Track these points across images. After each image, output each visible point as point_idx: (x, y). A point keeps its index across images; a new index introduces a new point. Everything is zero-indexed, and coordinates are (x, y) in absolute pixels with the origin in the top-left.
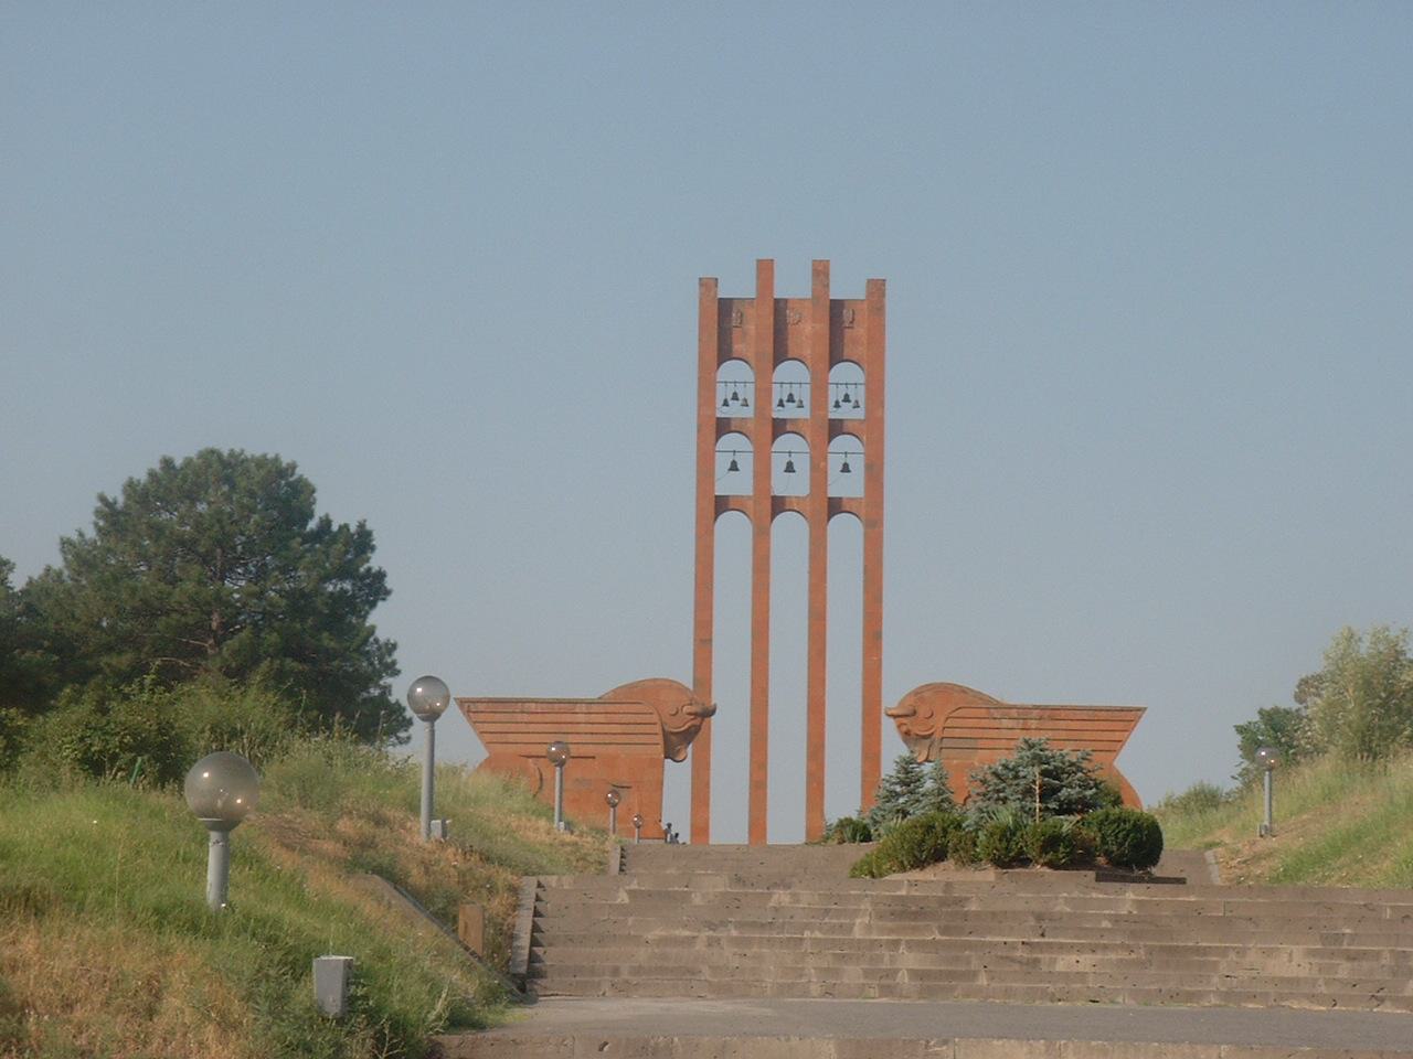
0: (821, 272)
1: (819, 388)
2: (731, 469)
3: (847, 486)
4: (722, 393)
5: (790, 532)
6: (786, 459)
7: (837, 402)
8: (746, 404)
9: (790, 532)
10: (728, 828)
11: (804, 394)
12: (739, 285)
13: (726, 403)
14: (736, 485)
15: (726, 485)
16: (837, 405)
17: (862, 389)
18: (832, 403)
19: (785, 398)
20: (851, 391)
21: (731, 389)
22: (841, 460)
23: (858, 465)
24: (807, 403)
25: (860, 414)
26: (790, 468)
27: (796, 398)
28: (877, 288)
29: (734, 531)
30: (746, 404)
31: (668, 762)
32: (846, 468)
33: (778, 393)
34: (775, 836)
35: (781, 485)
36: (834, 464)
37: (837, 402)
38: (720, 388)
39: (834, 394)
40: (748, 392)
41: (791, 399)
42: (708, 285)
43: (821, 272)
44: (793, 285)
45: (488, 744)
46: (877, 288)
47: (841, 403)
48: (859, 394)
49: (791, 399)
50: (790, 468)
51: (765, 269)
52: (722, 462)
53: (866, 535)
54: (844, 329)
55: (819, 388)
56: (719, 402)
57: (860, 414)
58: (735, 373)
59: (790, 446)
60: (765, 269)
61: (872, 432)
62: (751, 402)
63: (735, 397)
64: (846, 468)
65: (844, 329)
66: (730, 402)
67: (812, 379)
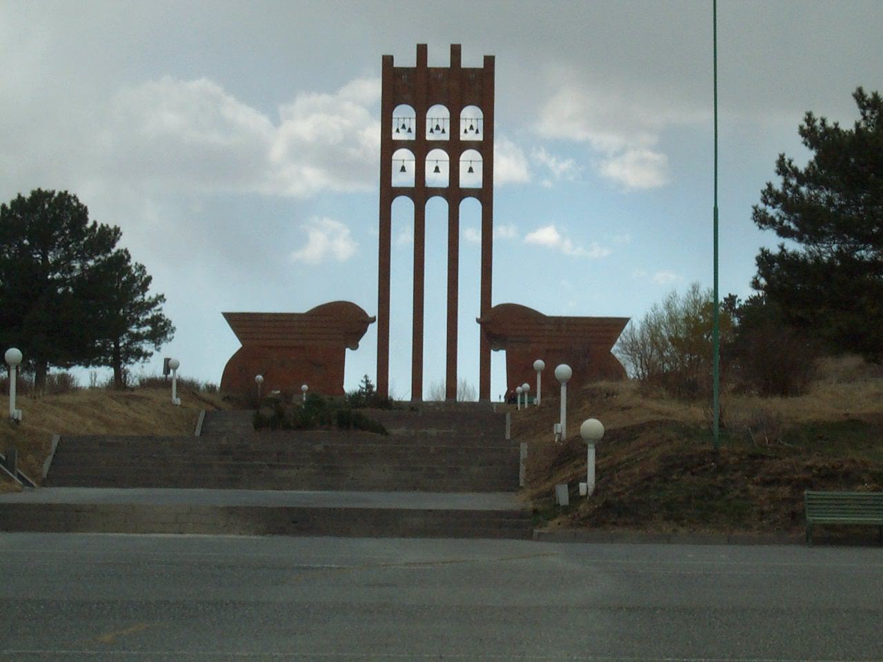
0: (456, 51)
5: (437, 208)
9: (437, 208)
10: (400, 390)
12: (406, 59)
14: (403, 179)
17: (482, 121)
19: (434, 128)
24: (447, 130)
25: (480, 137)
26: (437, 170)
27: (441, 129)
28: (489, 61)
29: (403, 208)
31: (348, 350)
32: (471, 170)
34: (426, 397)
39: (464, 125)
42: (387, 61)
43: (456, 51)
44: (439, 59)
45: (241, 340)
46: (489, 61)
47: (468, 131)
49: (438, 128)
51: (422, 50)
53: (483, 209)
54: (470, 86)
56: (394, 130)
57: (480, 137)
58: (404, 115)
60: (422, 50)
61: (486, 148)
64: (471, 170)
65: (470, 86)
66: (400, 130)
67: (450, 116)
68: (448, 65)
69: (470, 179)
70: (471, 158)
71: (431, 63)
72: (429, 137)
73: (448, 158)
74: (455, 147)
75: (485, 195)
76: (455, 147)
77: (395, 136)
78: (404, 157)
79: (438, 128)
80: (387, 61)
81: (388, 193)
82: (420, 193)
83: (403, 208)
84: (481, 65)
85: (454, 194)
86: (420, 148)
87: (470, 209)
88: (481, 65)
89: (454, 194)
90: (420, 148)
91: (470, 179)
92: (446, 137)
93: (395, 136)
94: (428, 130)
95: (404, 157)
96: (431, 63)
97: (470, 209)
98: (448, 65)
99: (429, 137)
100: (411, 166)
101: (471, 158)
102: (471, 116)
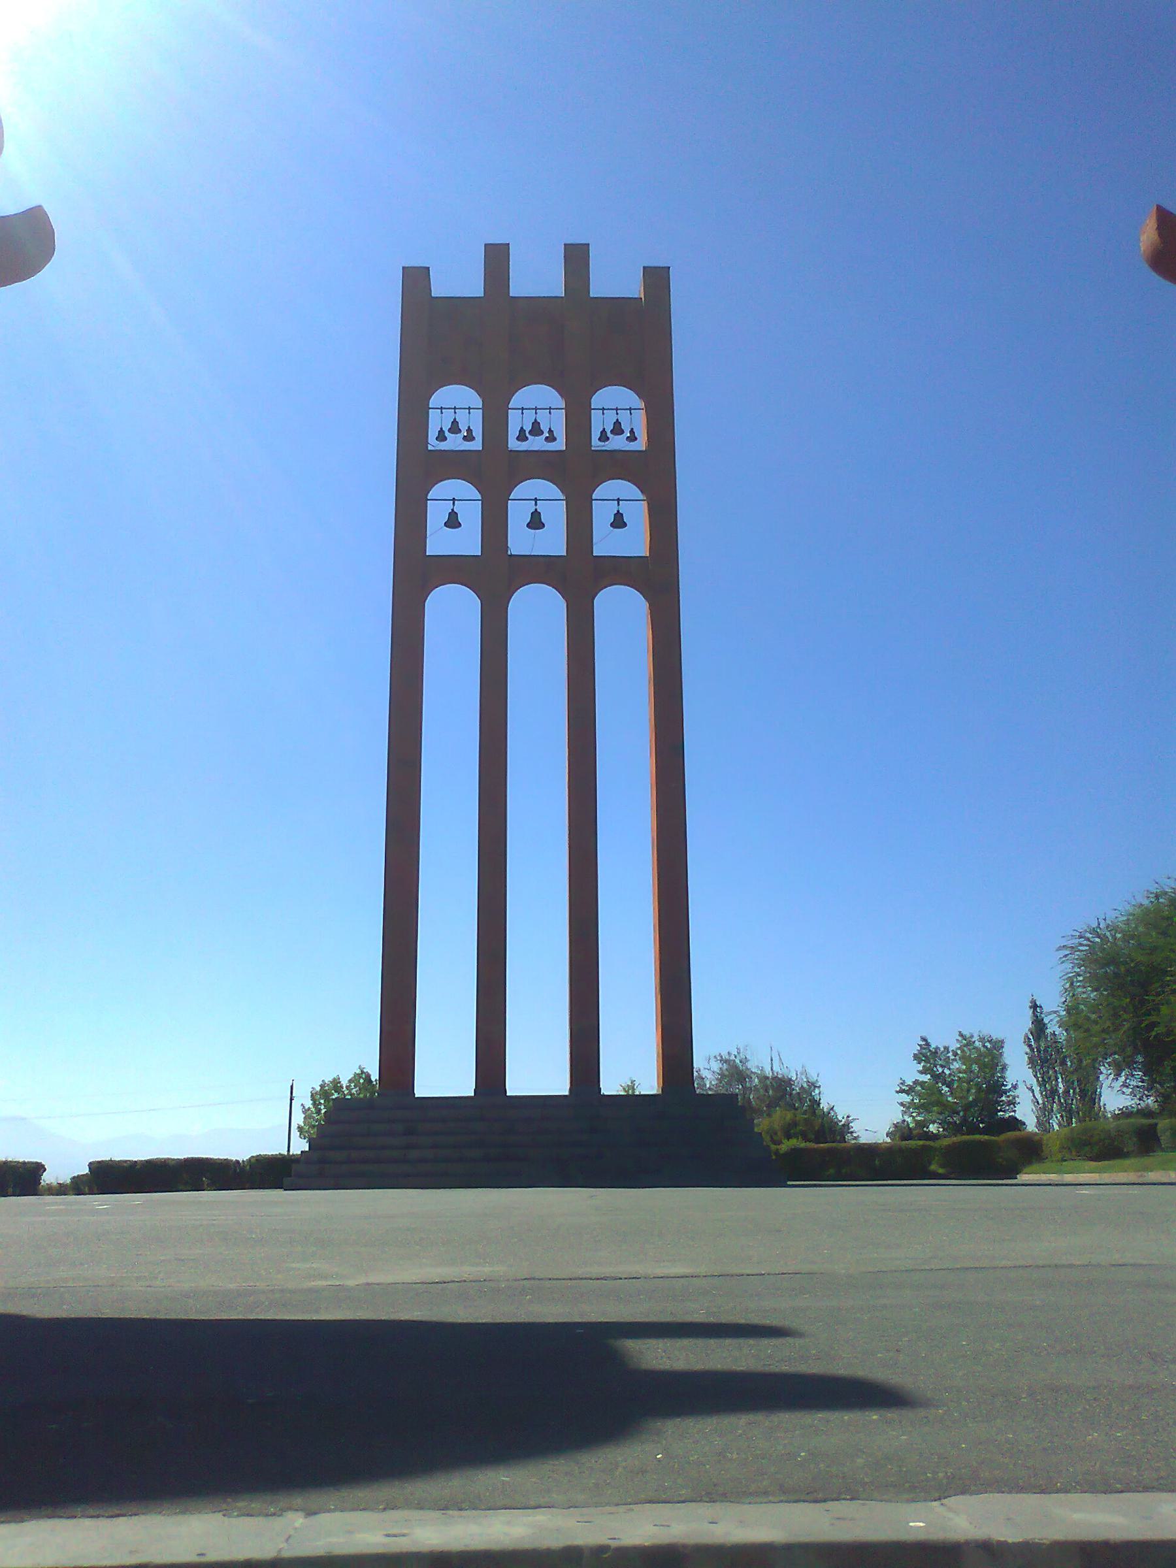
0: (577, 258)
3: (623, 537)
4: (436, 422)
5: (537, 613)
8: (469, 437)
9: (537, 613)
11: (557, 422)
12: (459, 279)
14: (454, 538)
15: (440, 542)
16: (604, 437)
19: (528, 428)
20: (624, 417)
21: (449, 417)
22: (613, 508)
23: (638, 513)
26: (536, 522)
27: (544, 427)
29: (452, 613)
30: (469, 437)
33: (515, 422)
35: (521, 541)
36: (602, 514)
38: (433, 415)
39: (599, 422)
40: (475, 422)
42: (415, 280)
43: (577, 258)
44: (537, 277)
46: (657, 279)
49: (536, 430)
50: (536, 522)
51: (497, 258)
52: (436, 514)
58: (456, 406)
60: (497, 258)
61: (654, 471)
62: (478, 433)
63: (455, 428)
66: (447, 434)
69: (623, 537)
72: (513, 444)
74: (578, 470)
75: (656, 575)
76: (578, 470)
77: (433, 444)
78: (453, 495)
79: (536, 430)
80: (415, 280)
81: (416, 574)
82: (495, 576)
83: (452, 613)
84: (632, 287)
85: (579, 576)
86: (495, 471)
87: (621, 613)
89: (579, 576)
90: (495, 471)
92: (560, 444)
93: (433, 444)
94: (513, 432)
95: (453, 495)
97: (621, 613)
99: (513, 444)
100: (472, 515)
102: (617, 408)
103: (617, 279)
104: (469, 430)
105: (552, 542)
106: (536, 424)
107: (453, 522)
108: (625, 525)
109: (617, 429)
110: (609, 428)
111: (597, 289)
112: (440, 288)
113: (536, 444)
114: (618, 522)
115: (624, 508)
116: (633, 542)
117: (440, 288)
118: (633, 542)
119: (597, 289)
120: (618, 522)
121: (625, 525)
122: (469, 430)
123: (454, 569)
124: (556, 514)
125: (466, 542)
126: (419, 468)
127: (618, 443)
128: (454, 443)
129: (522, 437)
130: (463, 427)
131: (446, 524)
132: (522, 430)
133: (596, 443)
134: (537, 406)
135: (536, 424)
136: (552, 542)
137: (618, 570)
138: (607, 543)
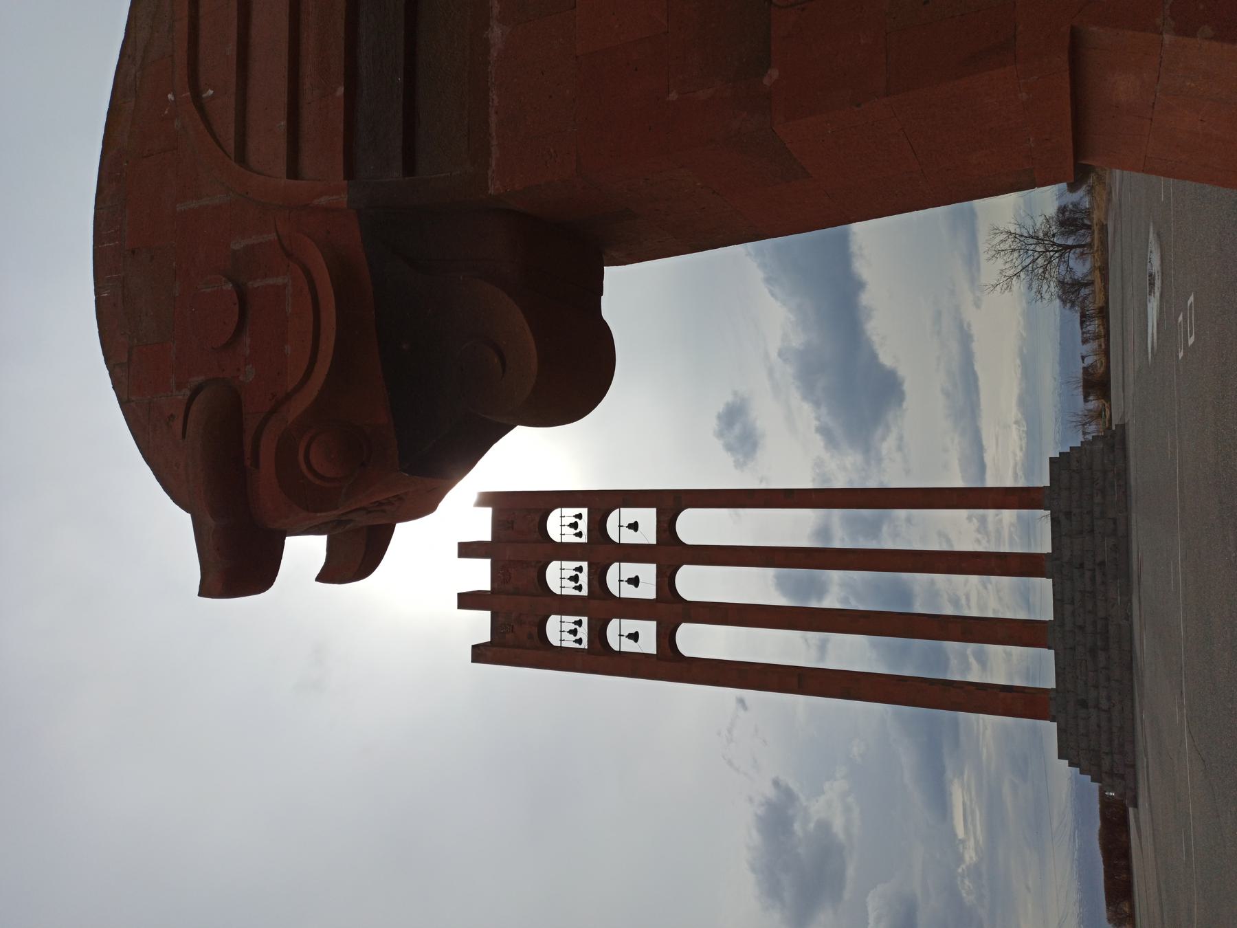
0: (468, 550)
1: (566, 552)
2: (636, 641)
5: (694, 583)
6: (624, 584)
7: (576, 535)
8: (579, 623)
9: (694, 583)
12: (479, 625)
13: (579, 641)
15: (648, 643)
16: (579, 535)
18: (577, 540)
19: (573, 584)
21: (566, 636)
22: (625, 530)
23: (630, 514)
24: (577, 564)
26: (635, 581)
27: (574, 573)
33: (569, 590)
35: (647, 590)
36: (629, 537)
37: (576, 535)
38: (565, 644)
39: (569, 537)
41: (575, 579)
43: (468, 550)
44: (479, 575)
48: (569, 513)
49: (575, 579)
50: (635, 581)
51: (468, 600)
52: (629, 646)
55: (566, 552)
57: (584, 511)
58: (560, 630)
59: (617, 577)
60: (468, 600)
61: (600, 503)
62: (577, 618)
63: (574, 632)
68: (486, 563)
70: (617, 525)
71: (485, 584)
73: (615, 566)
74: (599, 551)
75: (668, 504)
78: (617, 633)
80: (480, 654)
81: (669, 664)
82: (670, 610)
83: (695, 640)
84: (488, 512)
85: (670, 553)
86: (600, 606)
87: (695, 527)
88: (488, 512)
89: (670, 553)
91: (634, 526)
94: (576, 593)
95: (617, 633)
96: (485, 584)
97: (695, 527)
98: (486, 563)
99: (585, 592)
101: (617, 525)
102: (561, 526)
103: (481, 527)
104: (575, 623)
105: (648, 572)
106: (571, 579)
107: (634, 637)
108: (636, 523)
109: (574, 525)
110: (573, 531)
111: (486, 536)
112: (486, 638)
113: (584, 579)
114: (634, 526)
115: (625, 523)
116: (647, 518)
117: (486, 638)
118: (647, 518)
119: (486, 536)
120: (634, 526)
121: (636, 523)
122: (575, 623)
123: (666, 638)
124: (630, 569)
125: (648, 630)
126: (598, 658)
127: (583, 525)
128: (583, 632)
129: (579, 588)
130: (573, 627)
131: (636, 641)
132: (575, 588)
133: (584, 540)
134: (560, 577)
135: (571, 579)
136: (648, 572)
137: (666, 527)
138: (648, 534)
